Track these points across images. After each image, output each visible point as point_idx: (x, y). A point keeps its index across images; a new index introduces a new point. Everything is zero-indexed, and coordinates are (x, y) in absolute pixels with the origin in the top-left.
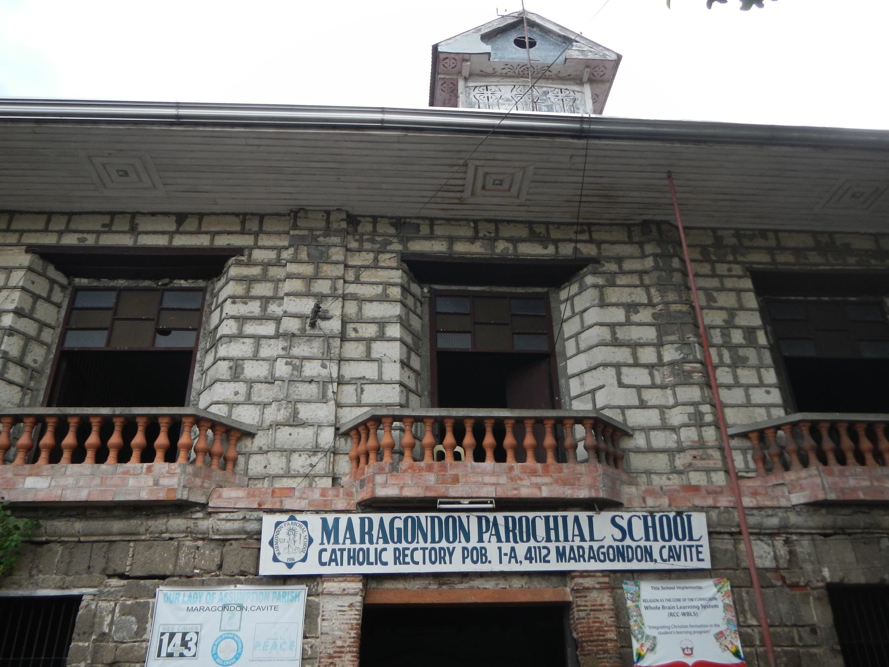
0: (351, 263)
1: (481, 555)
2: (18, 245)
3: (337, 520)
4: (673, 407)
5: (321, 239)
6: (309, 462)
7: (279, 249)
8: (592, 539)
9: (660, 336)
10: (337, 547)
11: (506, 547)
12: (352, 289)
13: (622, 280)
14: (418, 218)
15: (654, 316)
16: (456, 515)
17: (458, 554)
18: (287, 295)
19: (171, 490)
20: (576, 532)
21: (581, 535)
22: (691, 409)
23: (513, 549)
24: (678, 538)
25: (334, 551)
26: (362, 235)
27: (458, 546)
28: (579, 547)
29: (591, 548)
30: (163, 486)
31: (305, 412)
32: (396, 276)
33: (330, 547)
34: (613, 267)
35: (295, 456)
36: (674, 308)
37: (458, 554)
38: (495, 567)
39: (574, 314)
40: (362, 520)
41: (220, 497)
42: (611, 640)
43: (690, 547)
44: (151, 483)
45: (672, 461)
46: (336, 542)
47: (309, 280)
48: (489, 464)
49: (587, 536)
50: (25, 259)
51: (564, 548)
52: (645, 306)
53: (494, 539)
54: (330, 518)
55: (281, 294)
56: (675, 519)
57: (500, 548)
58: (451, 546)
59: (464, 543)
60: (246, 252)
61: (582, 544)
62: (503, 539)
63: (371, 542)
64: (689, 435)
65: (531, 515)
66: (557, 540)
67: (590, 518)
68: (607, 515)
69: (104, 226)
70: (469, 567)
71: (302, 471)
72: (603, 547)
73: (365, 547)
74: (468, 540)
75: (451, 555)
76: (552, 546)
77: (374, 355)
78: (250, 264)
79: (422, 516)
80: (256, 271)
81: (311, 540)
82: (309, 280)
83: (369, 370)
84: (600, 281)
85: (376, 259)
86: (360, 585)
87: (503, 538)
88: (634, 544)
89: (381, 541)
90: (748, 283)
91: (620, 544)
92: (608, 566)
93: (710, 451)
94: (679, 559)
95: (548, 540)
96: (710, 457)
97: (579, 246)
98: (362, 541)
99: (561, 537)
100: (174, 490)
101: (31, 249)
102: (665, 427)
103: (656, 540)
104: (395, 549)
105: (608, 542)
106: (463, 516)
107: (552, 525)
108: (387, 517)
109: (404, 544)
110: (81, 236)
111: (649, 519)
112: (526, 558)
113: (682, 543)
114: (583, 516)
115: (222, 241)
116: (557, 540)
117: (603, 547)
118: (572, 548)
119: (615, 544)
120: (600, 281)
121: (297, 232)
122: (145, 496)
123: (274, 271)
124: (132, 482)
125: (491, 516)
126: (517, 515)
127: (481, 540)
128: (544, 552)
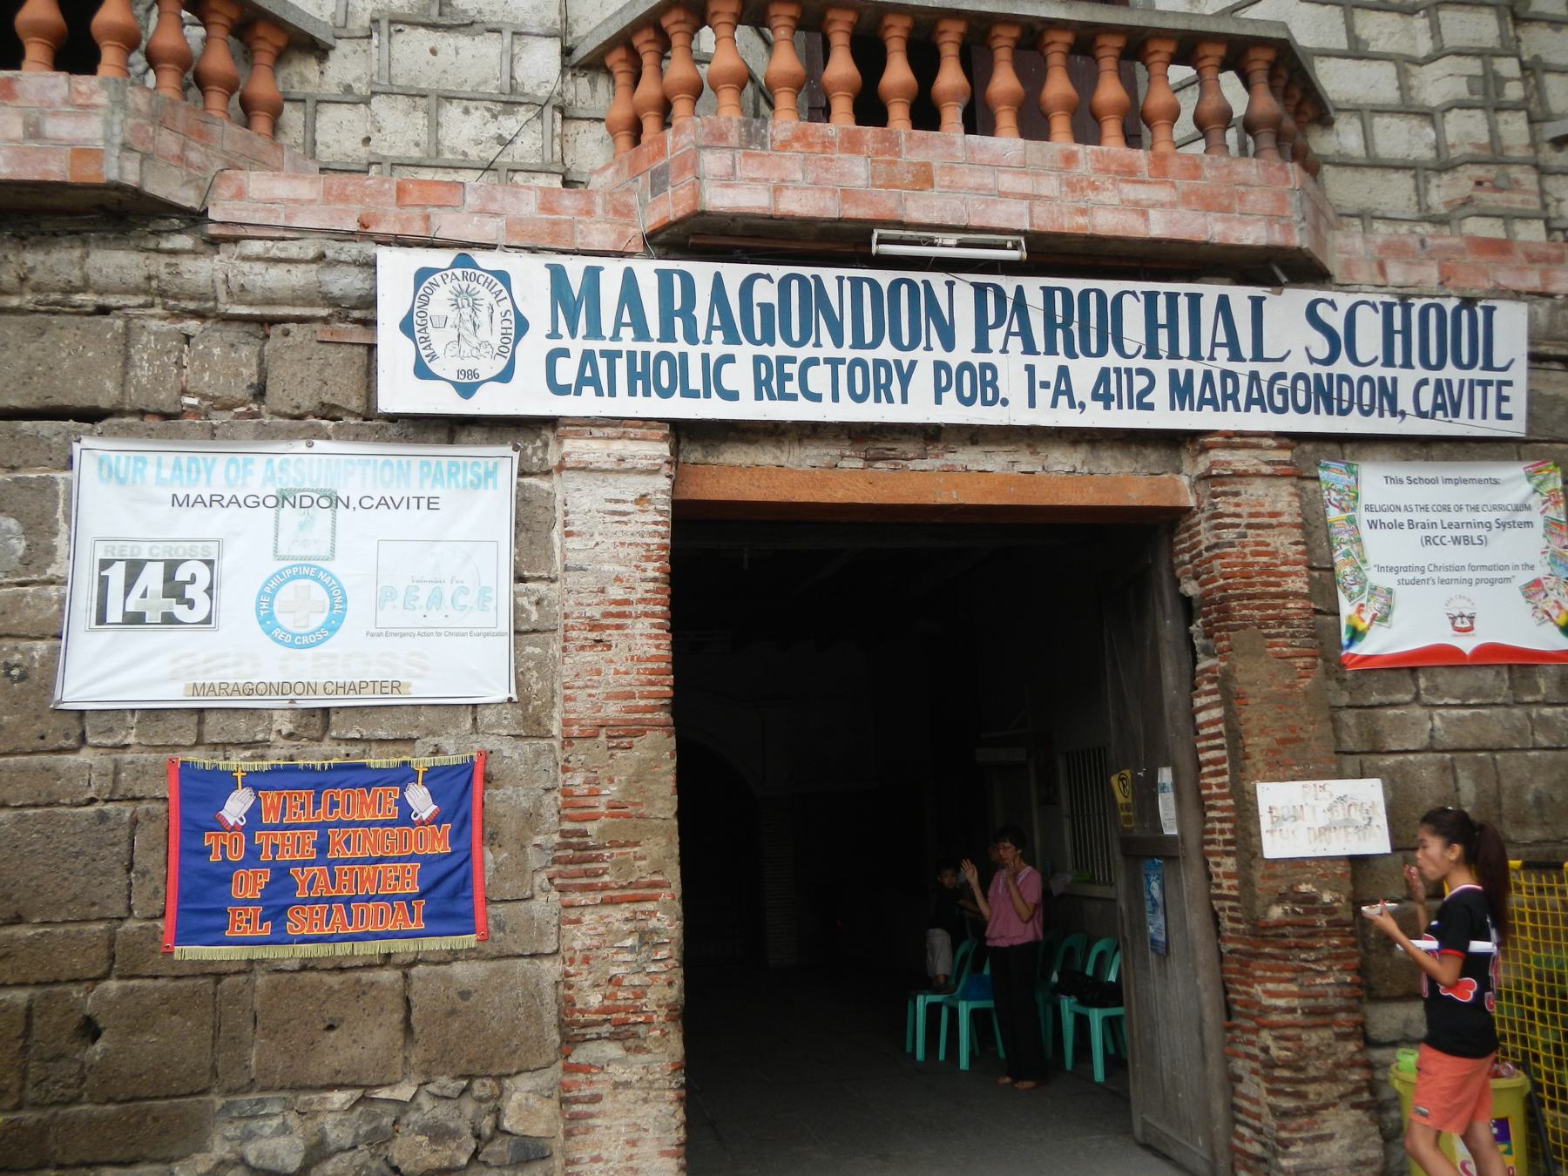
1: (985, 384)
3: (592, 275)
4: (1429, 59)
6: (492, 129)
8: (1258, 355)
10: (596, 346)
11: (1047, 368)
16: (918, 277)
17: (923, 380)
19: (82, 153)
20: (1222, 337)
21: (1233, 344)
22: (1474, 66)
23: (1063, 372)
24: (1458, 364)
25: (588, 356)
27: (924, 360)
28: (1226, 374)
29: (1254, 376)
30: (58, 141)
33: (577, 346)
35: (452, 112)
37: (923, 380)
38: (1017, 414)
40: (664, 277)
41: (240, 194)
42: (1296, 595)
43: (1485, 384)
44: (17, 130)
45: (1420, 192)
46: (595, 332)
48: (1006, 143)
49: (1246, 349)
51: (1189, 373)
53: (1016, 344)
54: (575, 268)
56: (1457, 313)
57: (1030, 369)
58: (905, 358)
59: (939, 353)
61: (1234, 366)
62: (1040, 344)
63: (691, 338)
64: (1466, 129)
65: (1111, 287)
66: (1174, 354)
67: (1257, 303)
68: (1297, 298)
70: (952, 412)
71: (474, 153)
72: (1282, 376)
73: (674, 349)
74: (949, 344)
75: (905, 379)
76: (1161, 368)
81: (522, 325)
86: (664, 449)
87: (1040, 344)
88: (1355, 373)
89: (718, 336)
91: (1324, 370)
92: (1293, 422)
93: (1515, 172)
94: (1456, 414)
95: (1153, 353)
96: (1514, 186)
98: (667, 335)
99: (1184, 347)
100: (94, 155)
102: (1408, 108)
103: (1407, 364)
104: (758, 360)
106: (938, 280)
107: (1162, 317)
108: (736, 274)
109: (780, 348)
111: (1397, 311)
112: (1095, 396)
113: (1468, 375)
114: (1240, 296)
116: (1174, 354)
117: (1282, 376)
118: (1208, 376)
119: (1311, 370)
125: (1009, 284)
126: (1076, 285)
127: (982, 345)
128: (1140, 383)
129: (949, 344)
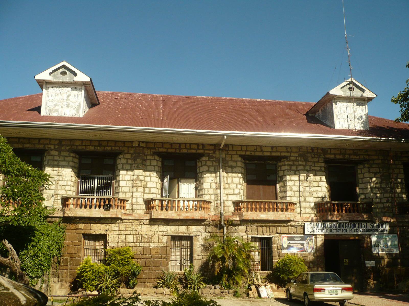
0: (313, 161)
1: (346, 231)
2: (236, 154)
4: (383, 198)
5: (306, 155)
7: (296, 157)
8: (367, 228)
9: (381, 181)
10: (319, 229)
11: (350, 229)
12: (314, 168)
13: (374, 166)
14: (327, 148)
15: (381, 176)
17: (341, 231)
18: (300, 170)
19: (289, 218)
22: (387, 199)
23: (352, 230)
26: (315, 153)
27: (341, 229)
29: (366, 229)
31: (307, 199)
32: (323, 164)
33: (318, 229)
34: (372, 162)
35: (306, 209)
36: (385, 174)
37: (341, 231)
38: (348, 233)
39: (361, 173)
41: (296, 218)
46: (319, 228)
47: (305, 166)
50: (240, 159)
52: (379, 173)
53: (348, 228)
55: (298, 169)
59: (343, 229)
60: (289, 158)
65: (355, 223)
68: (370, 223)
69: (255, 149)
70: (344, 233)
74: (343, 228)
75: (340, 231)
77: (320, 185)
78: (290, 161)
79: (335, 223)
80: (291, 163)
82: (305, 166)
83: (319, 189)
84: (369, 166)
85: (318, 160)
86: (323, 236)
90: (402, 167)
95: (358, 228)
97: (364, 156)
101: (240, 156)
102: (381, 203)
105: (370, 228)
106: (343, 223)
109: (332, 229)
110: (250, 152)
115: (283, 154)
119: (371, 229)
120: (369, 166)
121: (300, 153)
122: (284, 219)
123: (296, 163)
124: (281, 216)
125: (348, 223)
126: (353, 223)
127: (346, 228)
129: (343, 228)
